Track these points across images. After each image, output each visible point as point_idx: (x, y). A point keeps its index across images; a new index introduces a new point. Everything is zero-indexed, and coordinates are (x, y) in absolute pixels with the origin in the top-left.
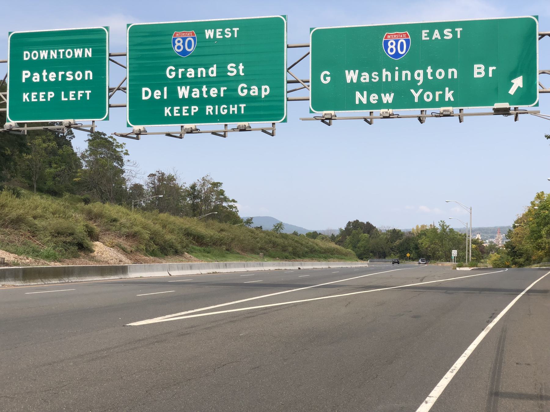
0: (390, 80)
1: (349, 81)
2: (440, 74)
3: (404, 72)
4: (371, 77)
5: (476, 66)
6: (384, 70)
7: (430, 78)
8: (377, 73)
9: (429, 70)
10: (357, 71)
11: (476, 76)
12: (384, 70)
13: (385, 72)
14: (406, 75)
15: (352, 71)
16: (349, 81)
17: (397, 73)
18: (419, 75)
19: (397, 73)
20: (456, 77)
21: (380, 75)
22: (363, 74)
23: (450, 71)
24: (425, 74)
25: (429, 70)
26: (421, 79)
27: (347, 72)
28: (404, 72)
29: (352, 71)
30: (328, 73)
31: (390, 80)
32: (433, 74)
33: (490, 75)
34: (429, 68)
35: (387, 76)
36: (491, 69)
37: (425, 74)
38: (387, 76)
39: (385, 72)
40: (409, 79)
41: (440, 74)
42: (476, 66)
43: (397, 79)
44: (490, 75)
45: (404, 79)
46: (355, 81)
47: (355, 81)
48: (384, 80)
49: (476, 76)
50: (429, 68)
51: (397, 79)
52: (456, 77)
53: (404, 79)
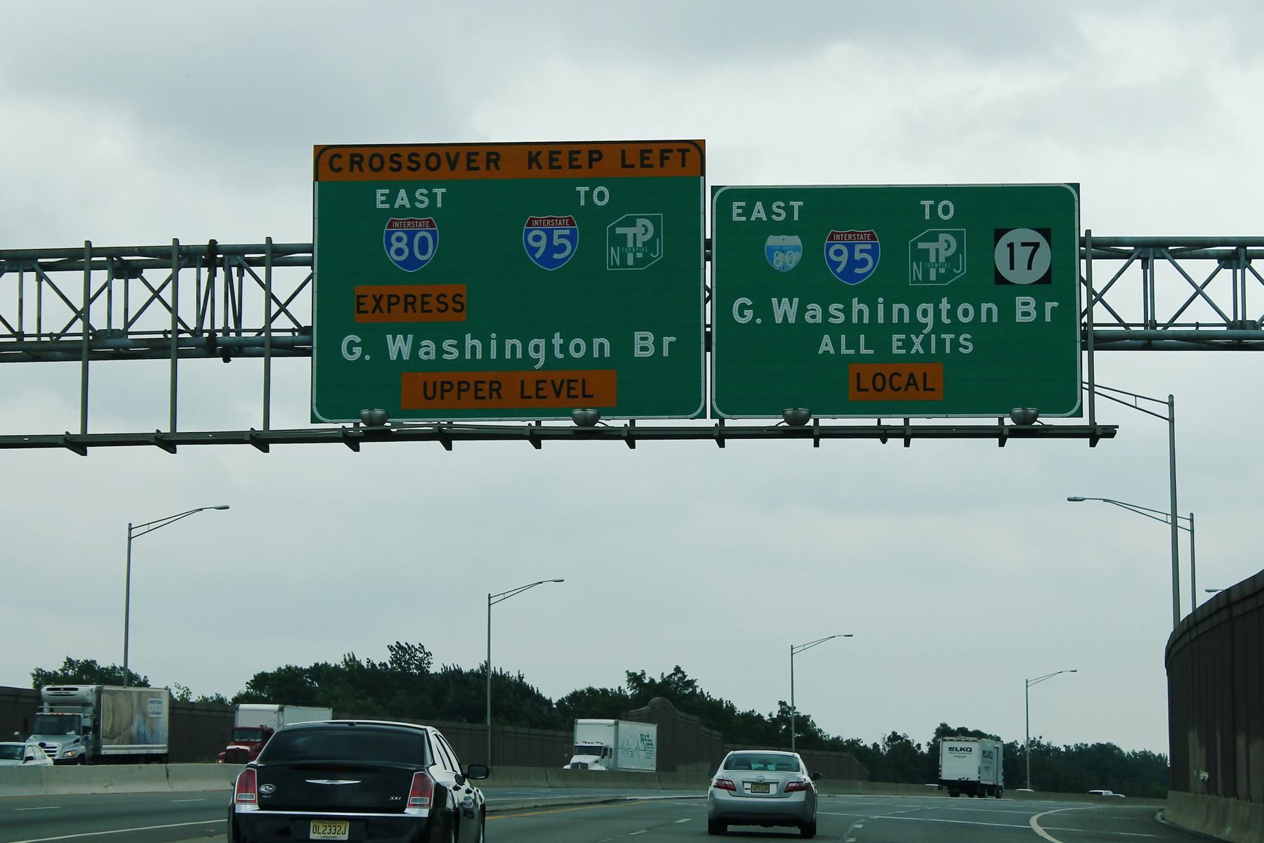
0: (479, 356)
1: (393, 356)
2: (577, 348)
3: (509, 343)
4: (440, 351)
5: (638, 335)
6: (468, 336)
7: (559, 356)
8: (454, 342)
9: (557, 340)
10: (410, 337)
11: (638, 353)
12: (468, 336)
13: (469, 341)
14: (514, 347)
15: (400, 337)
16: (393, 356)
17: (493, 344)
18: (537, 349)
19: (493, 344)
20: (607, 354)
21: (461, 347)
22: (423, 343)
23: (596, 341)
24: (550, 348)
25: (557, 340)
26: (541, 356)
27: (389, 337)
28: (509, 343)
29: (400, 337)
30: (358, 340)
31: (479, 356)
32: (564, 348)
33: (666, 354)
34: (557, 335)
35: (474, 348)
36: (667, 340)
37: (550, 348)
38: (474, 348)
39: (469, 341)
40: (519, 355)
41: (577, 348)
42: (638, 335)
43: (493, 355)
44: (666, 354)
45: (508, 356)
46: (406, 357)
47: (406, 357)
48: (468, 356)
49: (638, 353)
50: (557, 335)
51: (493, 355)
52: (607, 354)
53: (508, 356)
